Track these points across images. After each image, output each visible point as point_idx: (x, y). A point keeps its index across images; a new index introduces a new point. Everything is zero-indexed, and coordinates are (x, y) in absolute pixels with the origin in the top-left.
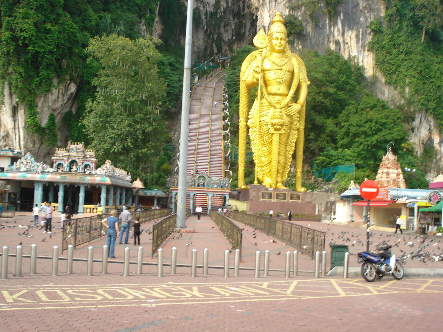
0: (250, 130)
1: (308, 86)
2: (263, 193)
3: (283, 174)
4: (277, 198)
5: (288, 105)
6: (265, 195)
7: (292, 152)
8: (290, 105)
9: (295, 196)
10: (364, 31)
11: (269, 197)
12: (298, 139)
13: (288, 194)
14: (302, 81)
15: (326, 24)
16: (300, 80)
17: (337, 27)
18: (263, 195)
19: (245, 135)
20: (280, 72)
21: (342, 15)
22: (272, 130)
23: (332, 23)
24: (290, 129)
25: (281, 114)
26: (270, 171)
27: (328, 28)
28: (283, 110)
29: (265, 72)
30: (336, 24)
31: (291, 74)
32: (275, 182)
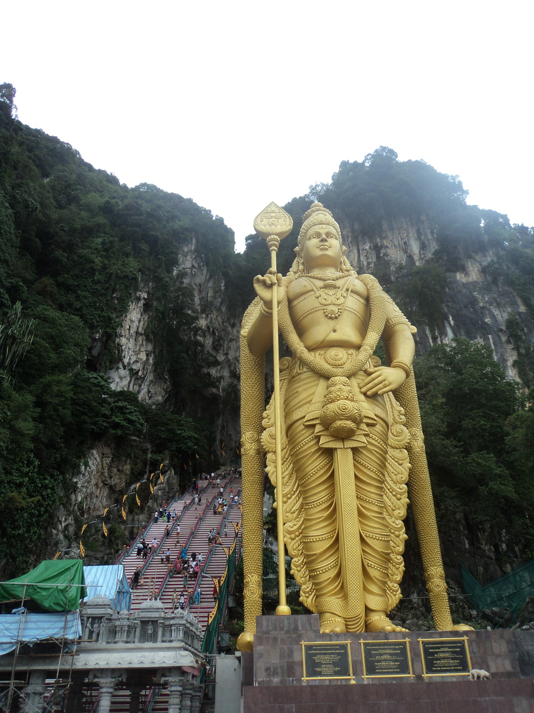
0: (269, 456)
1: (413, 335)
2: (309, 648)
3: (385, 583)
4: (371, 670)
5: (365, 371)
6: (317, 659)
7: (402, 512)
8: (372, 370)
9: (444, 654)
10: (497, 338)
11: (335, 664)
12: (412, 473)
13: (414, 646)
14: (394, 321)
15: (426, 335)
16: (387, 321)
17: (446, 339)
18: (309, 657)
19: (257, 478)
20: (331, 292)
21: (451, 318)
22: (325, 442)
23: (437, 334)
24: (385, 439)
25: (347, 388)
26: (339, 574)
27: (431, 341)
28: (354, 382)
29: (295, 303)
30: (443, 333)
31: (362, 301)
32: (361, 610)
